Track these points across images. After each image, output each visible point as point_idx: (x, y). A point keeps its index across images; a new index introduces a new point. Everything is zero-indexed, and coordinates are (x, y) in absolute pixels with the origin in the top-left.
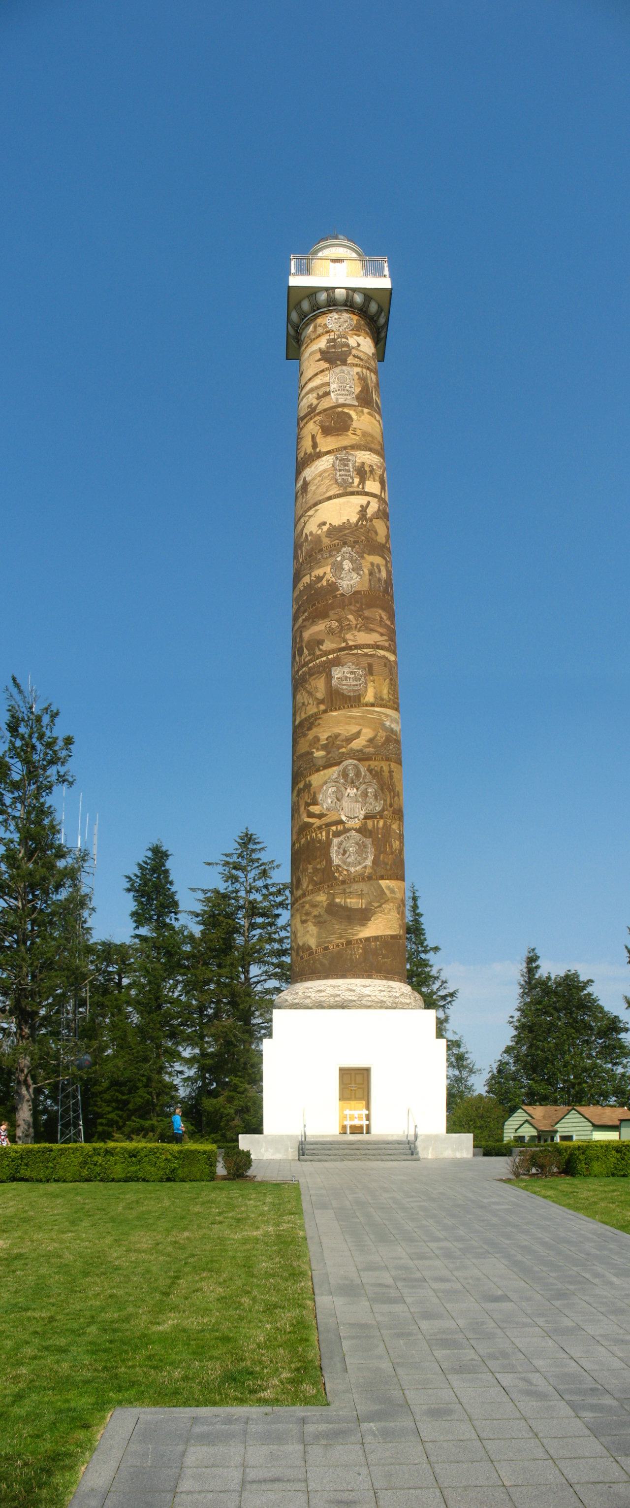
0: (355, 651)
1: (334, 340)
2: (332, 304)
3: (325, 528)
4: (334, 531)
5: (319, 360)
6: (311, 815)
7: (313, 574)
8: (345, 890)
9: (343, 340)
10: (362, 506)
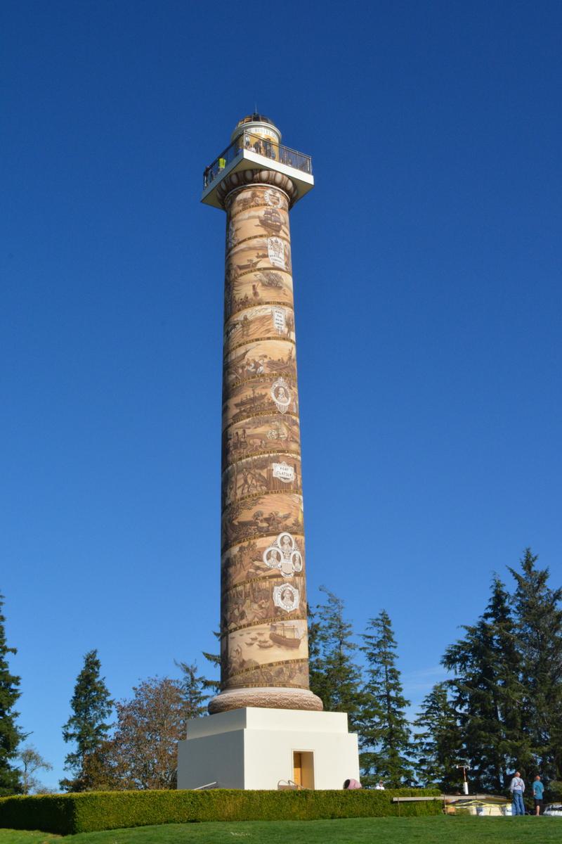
0: (287, 454)
1: (270, 214)
4: (272, 364)
5: (258, 226)
6: (258, 568)
7: (256, 392)
8: (283, 624)
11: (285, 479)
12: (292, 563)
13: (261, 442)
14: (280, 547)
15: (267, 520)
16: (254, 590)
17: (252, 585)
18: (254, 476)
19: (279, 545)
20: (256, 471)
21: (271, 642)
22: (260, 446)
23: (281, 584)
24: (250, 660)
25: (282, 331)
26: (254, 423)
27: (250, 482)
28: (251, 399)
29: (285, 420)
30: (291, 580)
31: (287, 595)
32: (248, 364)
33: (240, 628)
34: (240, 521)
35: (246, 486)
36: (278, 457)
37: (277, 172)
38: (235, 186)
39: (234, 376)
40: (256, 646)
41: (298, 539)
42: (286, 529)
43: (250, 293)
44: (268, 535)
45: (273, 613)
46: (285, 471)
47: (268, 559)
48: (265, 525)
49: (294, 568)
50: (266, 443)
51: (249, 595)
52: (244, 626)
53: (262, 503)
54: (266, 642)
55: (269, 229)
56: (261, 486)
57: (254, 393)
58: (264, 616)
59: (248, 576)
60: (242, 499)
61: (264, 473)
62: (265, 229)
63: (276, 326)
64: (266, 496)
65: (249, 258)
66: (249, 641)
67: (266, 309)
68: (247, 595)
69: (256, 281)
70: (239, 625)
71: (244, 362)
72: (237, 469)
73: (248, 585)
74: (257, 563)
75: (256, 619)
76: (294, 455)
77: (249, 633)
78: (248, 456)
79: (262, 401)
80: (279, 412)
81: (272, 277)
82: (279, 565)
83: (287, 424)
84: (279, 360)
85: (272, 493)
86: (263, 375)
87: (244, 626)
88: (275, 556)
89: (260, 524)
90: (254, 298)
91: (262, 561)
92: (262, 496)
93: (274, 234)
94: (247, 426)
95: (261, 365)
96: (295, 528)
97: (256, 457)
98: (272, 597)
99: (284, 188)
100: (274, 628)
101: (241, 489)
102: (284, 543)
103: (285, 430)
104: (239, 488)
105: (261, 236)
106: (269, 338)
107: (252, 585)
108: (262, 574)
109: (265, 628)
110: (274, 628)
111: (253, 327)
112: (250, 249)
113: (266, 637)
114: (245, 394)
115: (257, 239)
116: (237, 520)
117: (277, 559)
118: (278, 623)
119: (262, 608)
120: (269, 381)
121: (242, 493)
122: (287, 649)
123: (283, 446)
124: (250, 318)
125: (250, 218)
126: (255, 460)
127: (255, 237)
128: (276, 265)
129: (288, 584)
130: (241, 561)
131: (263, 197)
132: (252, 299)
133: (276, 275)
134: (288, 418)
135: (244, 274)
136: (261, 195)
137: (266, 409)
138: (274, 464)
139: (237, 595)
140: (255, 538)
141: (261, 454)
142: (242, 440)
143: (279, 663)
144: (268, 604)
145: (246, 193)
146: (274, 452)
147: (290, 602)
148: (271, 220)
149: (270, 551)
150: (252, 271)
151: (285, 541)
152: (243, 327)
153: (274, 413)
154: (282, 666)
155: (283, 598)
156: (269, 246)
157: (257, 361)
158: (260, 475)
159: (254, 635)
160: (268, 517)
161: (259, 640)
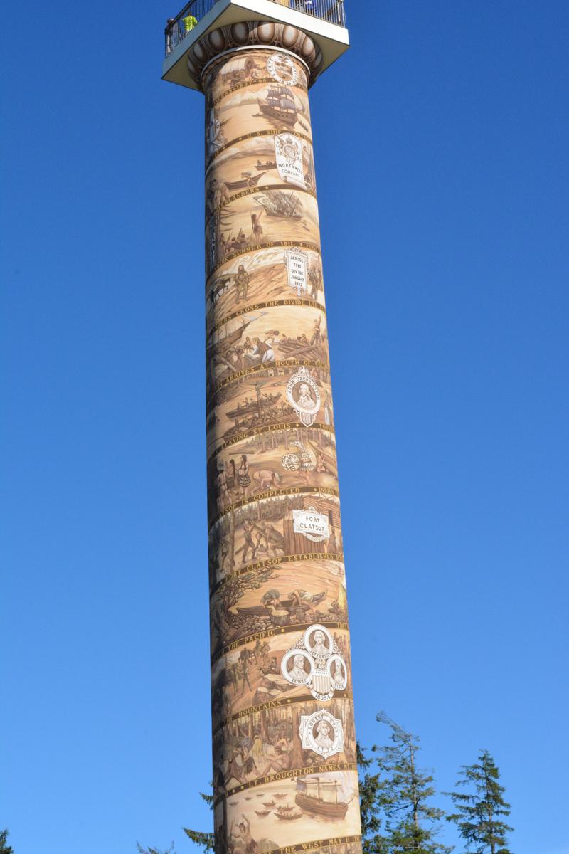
0: (317, 495)
1: (278, 95)
2: (277, 41)
3: (278, 339)
4: (287, 345)
5: (258, 115)
6: (273, 685)
7: (263, 391)
8: (318, 779)
9: (288, 97)
10: (316, 321)
11: (314, 535)
12: (329, 675)
13: (273, 475)
14: (309, 648)
15: (286, 605)
16: (268, 722)
17: (264, 714)
18: (262, 533)
19: (307, 646)
20: (266, 523)
21: (297, 810)
22: (272, 483)
23: (312, 712)
24: (264, 840)
25: (302, 290)
26: (261, 443)
27: (255, 541)
28: (254, 405)
29: (310, 438)
30: (328, 704)
31: (323, 730)
32: (248, 347)
33: (246, 786)
35: (250, 549)
36: (302, 499)
37: (287, 24)
38: (217, 50)
39: (226, 367)
40: (272, 816)
41: (338, 636)
42: (318, 618)
43: (248, 228)
44: (288, 630)
45: (300, 761)
46: (313, 523)
47: (289, 669)
48: (283, 613)
49: (333, 683)
50: (281, 477)
51: (260, 731)
52: (253, 783)
54: (289, 809)
55: (276, 121)
56: (274, 548)
57: (258, 394)
58: (285, 766)
59: (256, 700)
60: (244, 570)
61: (279, 527)
62: (270, 121)
63: (293, 281)
64: (283, 566)
65: (245, 171)
66: (262, 808)
67: (275, 254)
68: (256, 732)
69: (257, 208)
70: (244, 782)
71: (241, 343)
72: (234, 523)
73: (257, 715)
74: (271, 677)
75: (272, 772)
76: (328, 496)
77: (262, 795)
78: (251, 500)
79: (272, 407)
80: (301, 425)
81: (284, 201)
82: (308, 680)
83: (315, 444)
84: (299, 338)
85: (293, 559)
86: (272, 364)
87: (253, 783)
88: (301, 665)
89: (275, 613)
90: (254, 236)
91: (279, 673)
92: (275, 566)
93: (285, 128)
95: (270, 348)
96: (333, 617)
97: (264, 501)
98: (298, 733)
99: (300, 52)
100: (303, 785)
102: (316, 642)
103: (311, 454)
104: (237, 553)
105: (264, 133)
106: (281, 303)
107: (264, 714)
108: (280, 695)
109: (287, 787)
110: (303, 785)
111: (254, 285)
112: (246, 154)
113: (290, 800)
114: (245, 396)
115: (258, 138)
116: (236, 607)
117: (305, 670)
118: (309, 778)
119: (281, 752)
120: (283, 373)
121: (244, 562)
122: (326, 821)
123: (310, 481)
124: (249, 269)
125: (244, 103)
126: (263, 506)
127: (255, 135)
128: (289, 180)
129: (324, 711)
130: (245, 674)
131: (264, 68)
132: (251, 238)
133: (290, 197)
134: (317, 434)
135: (236, 196)
136: (262, 65)
137: (279, 420)
138: (295, 511)
139: (240, 732)
140: (266, 636)
141: (273, 495)
142: (241, 472)
143: (313, 845)
144: (292, 745)
145: (237, 61)
146: (294, 491)
147: (328, 741)
148: (279, 105)
149: (293, 657)
150: (249, 192)
151: (317, 640)
152: (238, 284)
153: (293, 426)
154: (317, 849)
155: (316, 734)
156: (277, 150)
157: (262, 340)
158: (272, 530)
159: (268, 797)
160: (288, 599)
161: (277, 806)
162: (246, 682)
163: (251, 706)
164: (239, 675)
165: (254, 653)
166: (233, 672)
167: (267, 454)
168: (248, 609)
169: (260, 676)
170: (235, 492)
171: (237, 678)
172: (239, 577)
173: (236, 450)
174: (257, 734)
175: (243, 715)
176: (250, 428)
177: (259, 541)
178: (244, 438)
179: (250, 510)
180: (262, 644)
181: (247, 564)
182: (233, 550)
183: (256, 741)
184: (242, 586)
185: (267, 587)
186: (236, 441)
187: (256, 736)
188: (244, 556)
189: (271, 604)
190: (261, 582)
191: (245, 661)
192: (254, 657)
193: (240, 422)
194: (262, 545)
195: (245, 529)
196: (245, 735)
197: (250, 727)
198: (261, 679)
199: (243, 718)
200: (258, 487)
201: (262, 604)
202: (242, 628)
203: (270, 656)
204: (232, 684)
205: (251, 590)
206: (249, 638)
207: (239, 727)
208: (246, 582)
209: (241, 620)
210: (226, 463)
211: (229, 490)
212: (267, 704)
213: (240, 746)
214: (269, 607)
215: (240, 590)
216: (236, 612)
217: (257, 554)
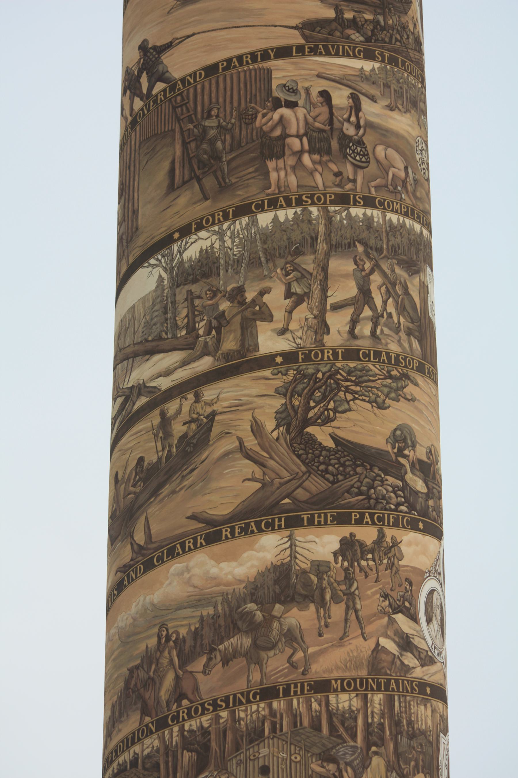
6: (406, 643)
16: (398, 724)
17: (390, 702)
27: (378, 301)
34: (340, 433)
35: (367, 312)
53: (412, 400)
68: (374, 738)
94: (365, 87)
101: (347, 313)
116: (328, 429)
130: (351, 596)
140: (396, 525)
162: (352, 616)
163: (363, 673)
164: (333, 590)
165: (372, 551)
166: (315, 579)
167: (395, 115)
168: (362, 446)
169: (383, 612)
170: (334, 168)
171: (328, 597)
172: (339, 364)
173: (337, 73)
174: (376, 745)
175: (343, 690)
176: (368, 40)
177: (385, 303)
178: (355, 56)
179: (368, 221)
180: (388, 539)
181: (359, 343)
182: (324, 297)
183: (376, 760)
184: (347, 390)
185: (398, 414)
186: (337, 55)
187: (374, 749)
188: (354, 322)
189: (405, 457)
190: (387, 396)
191: (352, 566)
192: (371, 563)
193: (348, 15)
194: (390, 315)
195: (356, 263)
196: (345, 735)
197: (360, 721)
198: (386, 619)
199: (344, 697)
200: (383, 182)
201: (389, 448)
202: (347, 483)
203: (403, 574)
204: (312, 607)
205: (368, 406)
206: (362, 515)
207: (330, 715)
208: (357, 384)
209: (343, 465)
210: (307, 90)
211: (316, 157)
212: (397, 681)
213: (333, 760)
214: (402, 460)
215: (341, 394)
216: (330, 444)
217: (382, 331)
